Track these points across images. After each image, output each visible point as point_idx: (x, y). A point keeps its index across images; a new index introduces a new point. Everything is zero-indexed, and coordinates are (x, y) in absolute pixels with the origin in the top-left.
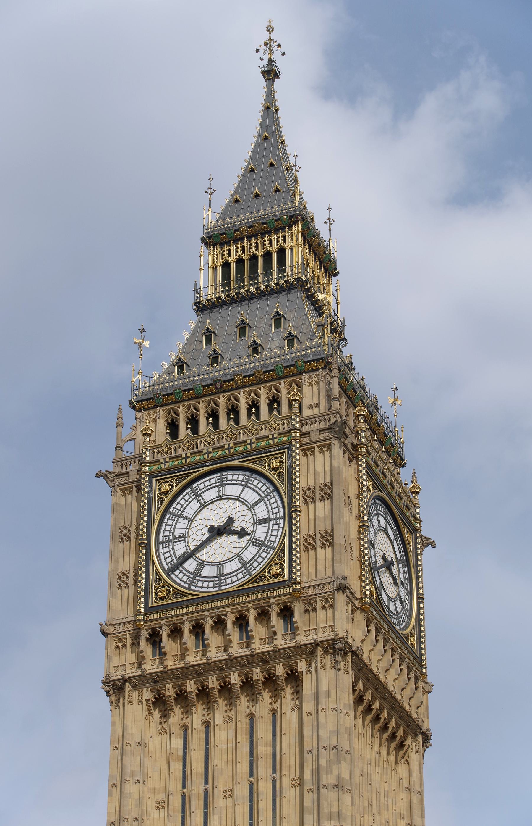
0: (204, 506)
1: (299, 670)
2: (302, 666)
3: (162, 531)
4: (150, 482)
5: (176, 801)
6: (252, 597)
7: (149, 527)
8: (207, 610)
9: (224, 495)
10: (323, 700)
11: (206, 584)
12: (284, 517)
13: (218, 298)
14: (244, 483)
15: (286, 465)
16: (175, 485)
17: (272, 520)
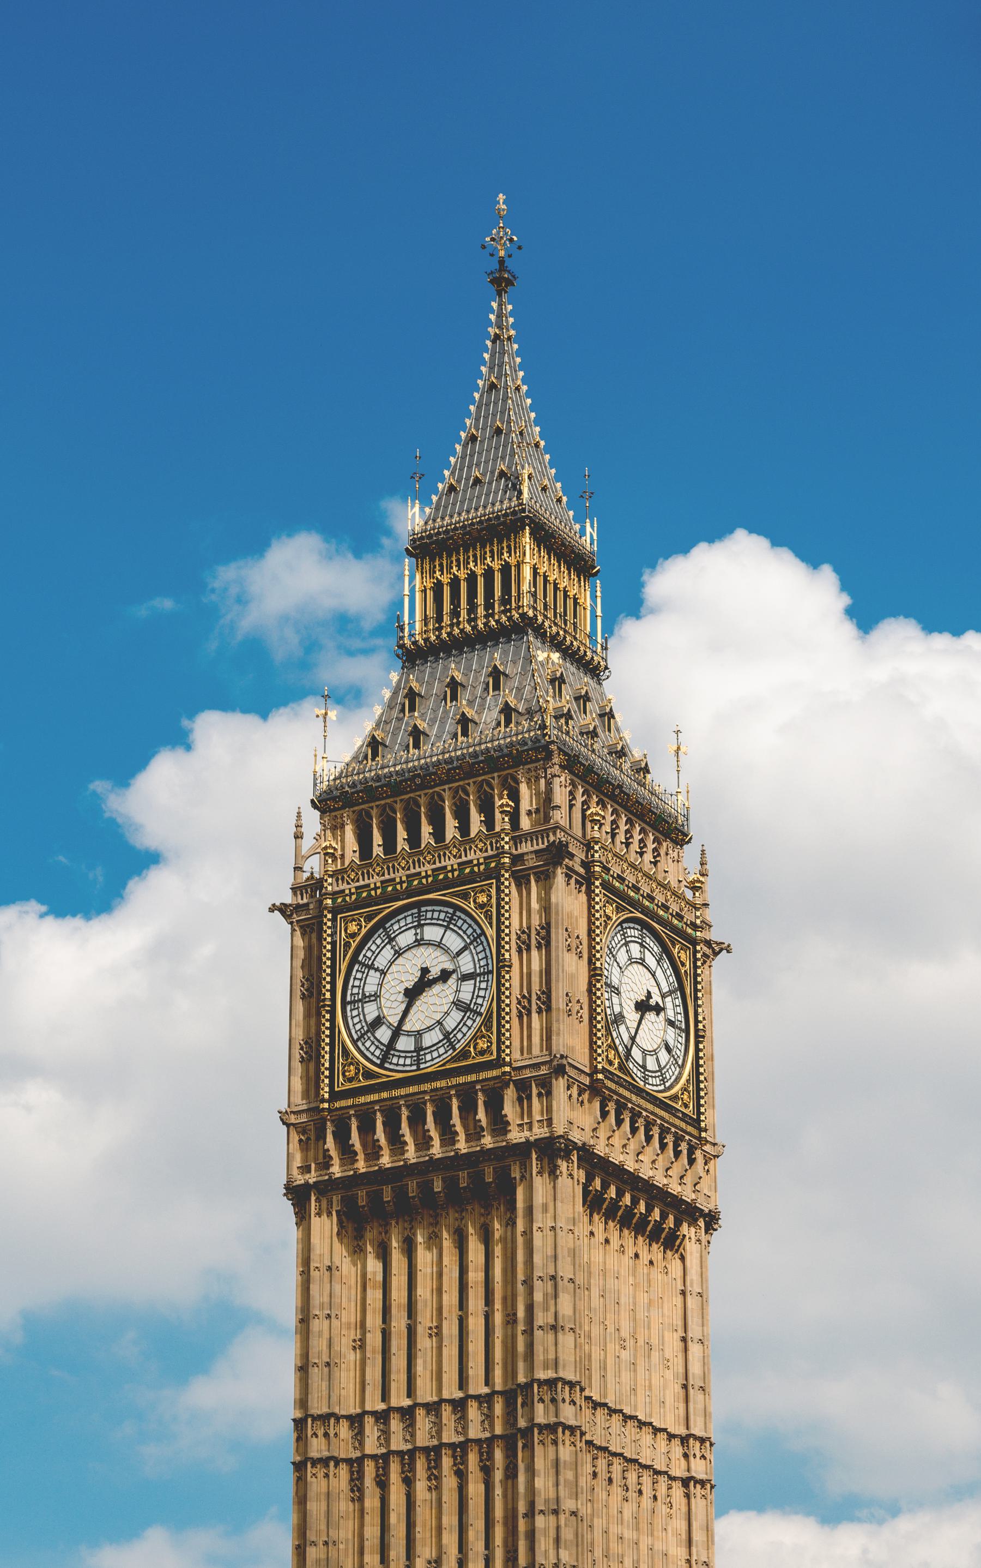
0: (398, 953)
1: (513, 1176)
2: (516, 1173)
3: (350, 987)
4: (334, 920)
5: (374, 1340)
6: (454, 1081)
7: (333, 983)
8: (402, 1097)
9: (422, 939)
10: (538, 1214)
11: (401, 1061)
12: (492, 972)
13: (426, 640)
14: (445, 924)
15: (494, 901)
16: (363, 924)
17: (479, 975)
